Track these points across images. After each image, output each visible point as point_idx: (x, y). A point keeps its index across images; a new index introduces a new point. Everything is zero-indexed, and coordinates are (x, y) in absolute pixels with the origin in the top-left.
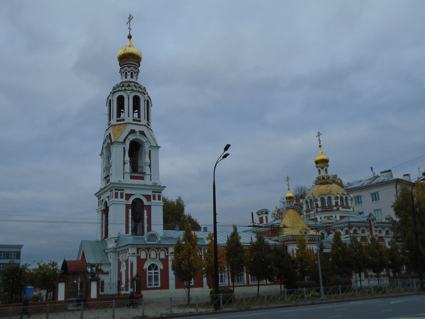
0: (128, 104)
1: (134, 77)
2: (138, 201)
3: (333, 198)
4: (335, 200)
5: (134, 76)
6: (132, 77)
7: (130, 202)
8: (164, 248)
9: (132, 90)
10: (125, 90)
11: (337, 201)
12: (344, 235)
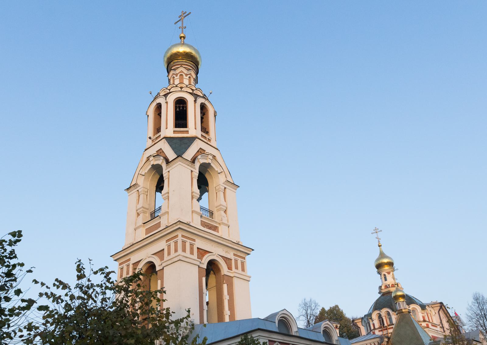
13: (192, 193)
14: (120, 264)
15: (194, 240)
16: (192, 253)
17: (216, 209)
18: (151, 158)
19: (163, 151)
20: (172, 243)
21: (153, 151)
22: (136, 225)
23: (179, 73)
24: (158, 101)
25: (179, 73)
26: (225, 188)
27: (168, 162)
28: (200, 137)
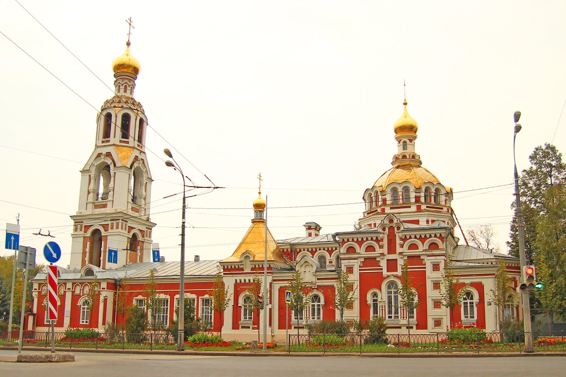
0: (117, 122)
1: (129, 92)
2: (97, 231)
3: (412, 189)
4: (416, 193)
5: (128, 90)
6: (125, 91)
7: (89, 234)
8: (79, 283)
9: (122, 107)
10: (115, 107)
11: (418, 194)
12: (344, 254)
13: (128, 189)
14: (75, 223)
15: (127, 222)
16: (125, 230)
17: (139, 196)
18: (103, 157)
19: (111, 155)
20: (115, 222)
21: (104, 151)
22: (87, 201)
23: (124, 84)
24: (109, 111)
25: (124, 84)
26: (146, 183)
27: (115, 165)
28: (136, 146)
